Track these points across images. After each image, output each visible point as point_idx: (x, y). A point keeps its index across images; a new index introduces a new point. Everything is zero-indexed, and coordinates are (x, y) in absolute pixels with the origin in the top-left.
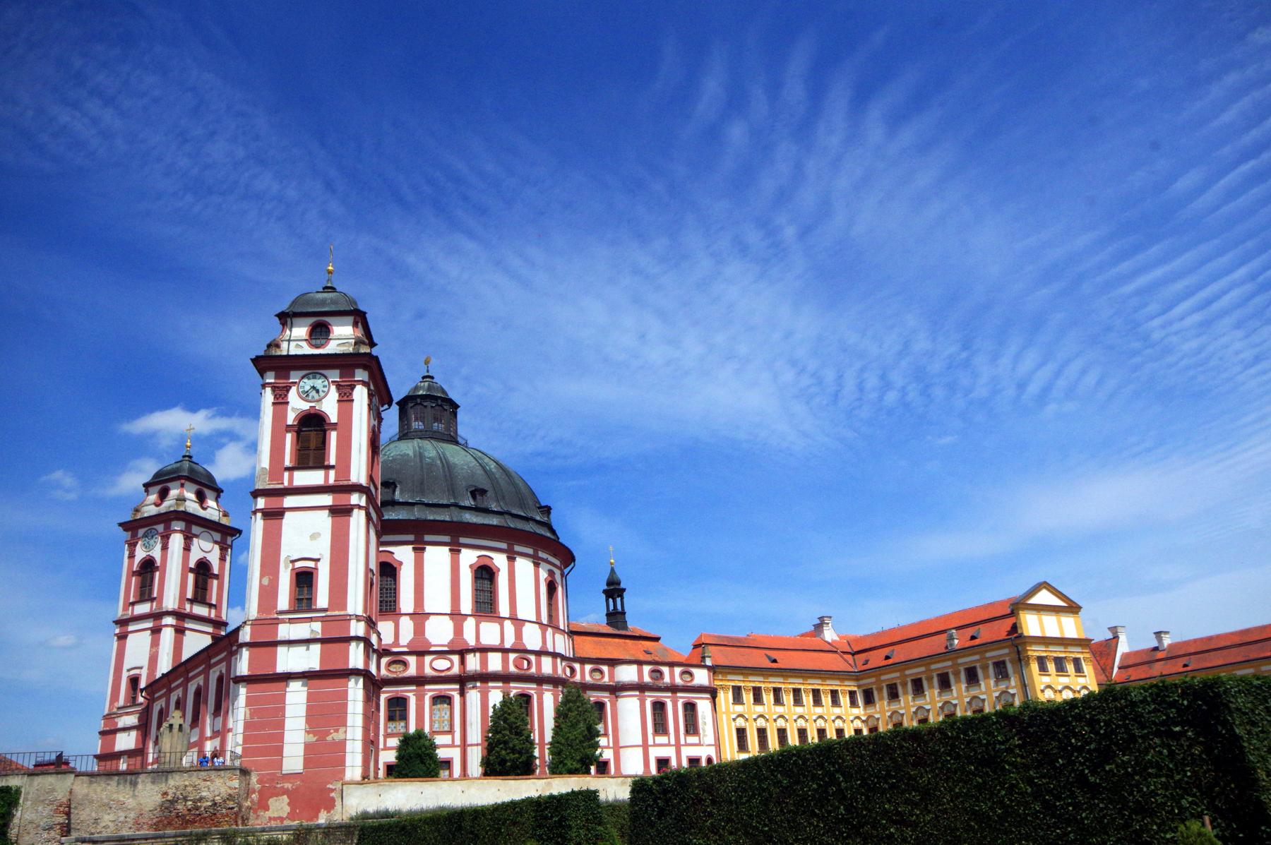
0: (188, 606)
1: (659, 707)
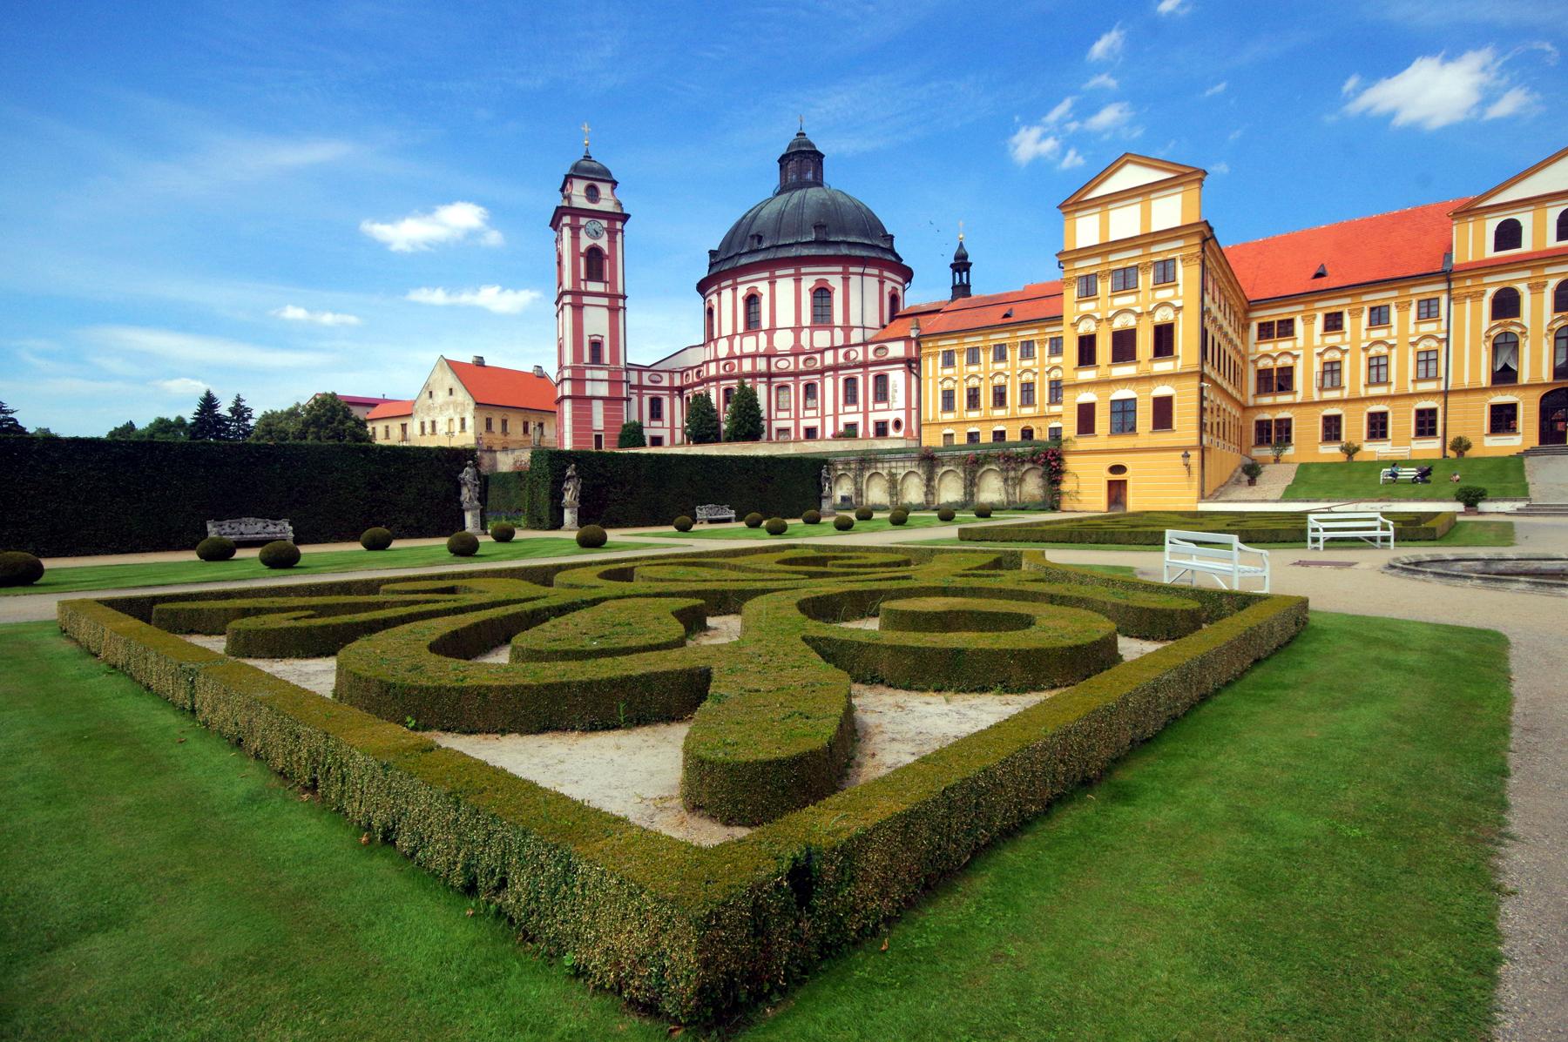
1: (850, 383)
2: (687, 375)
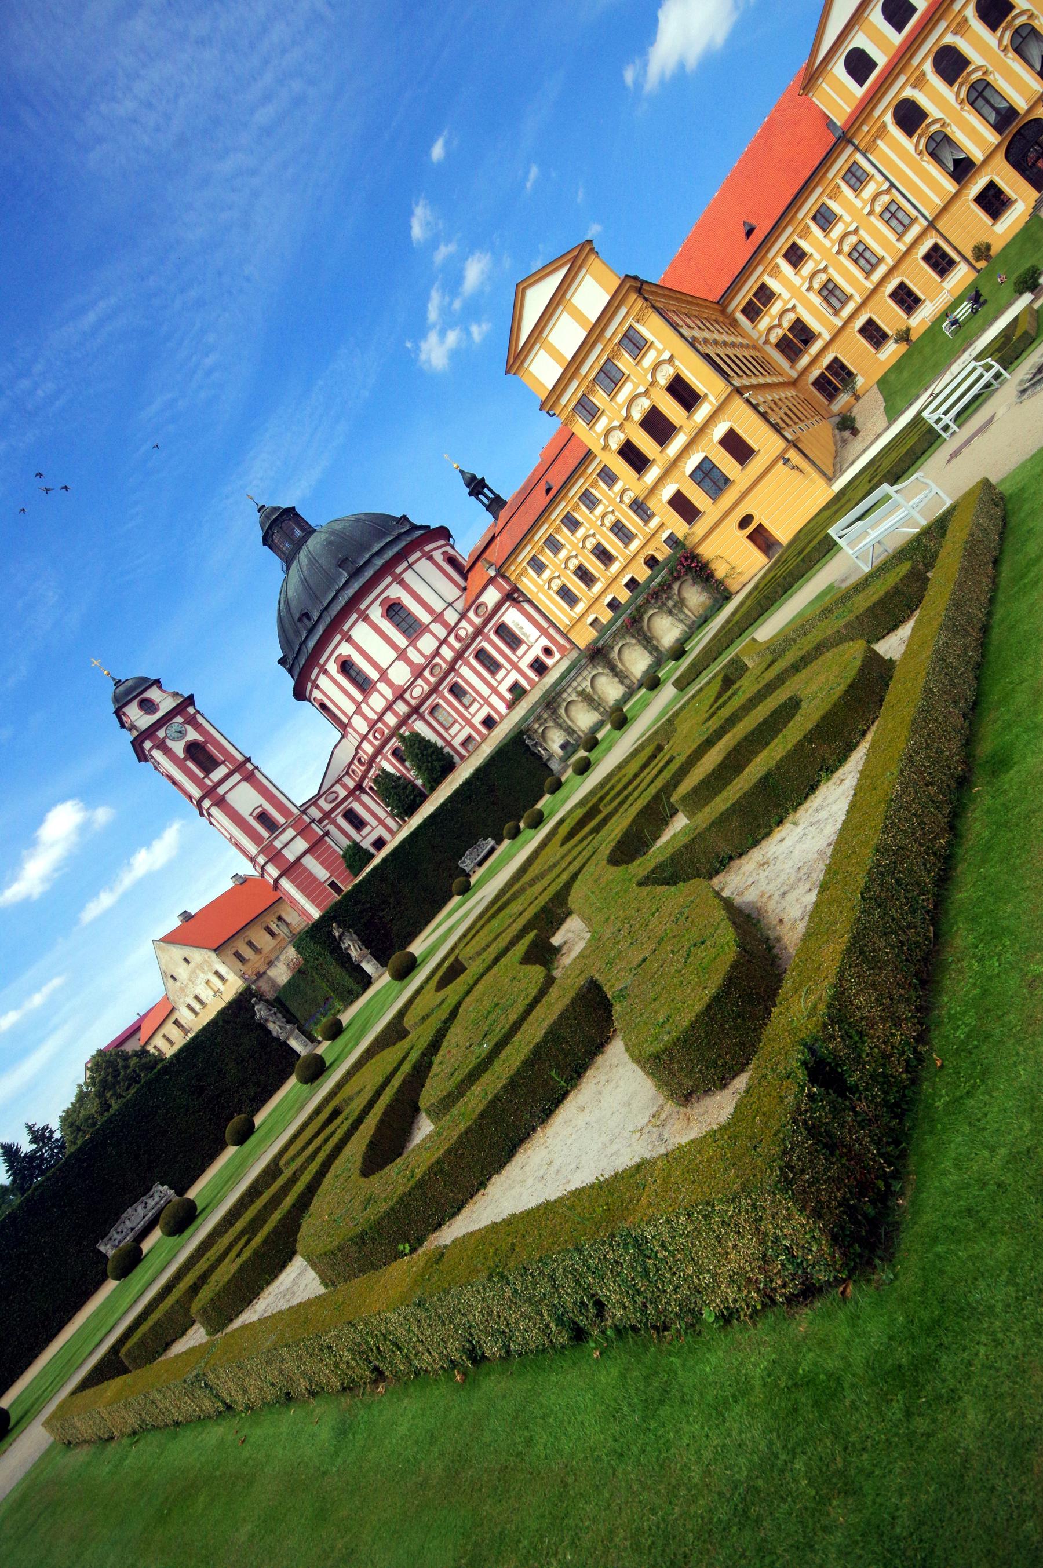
1: (482, 656)
2: (353, 771)
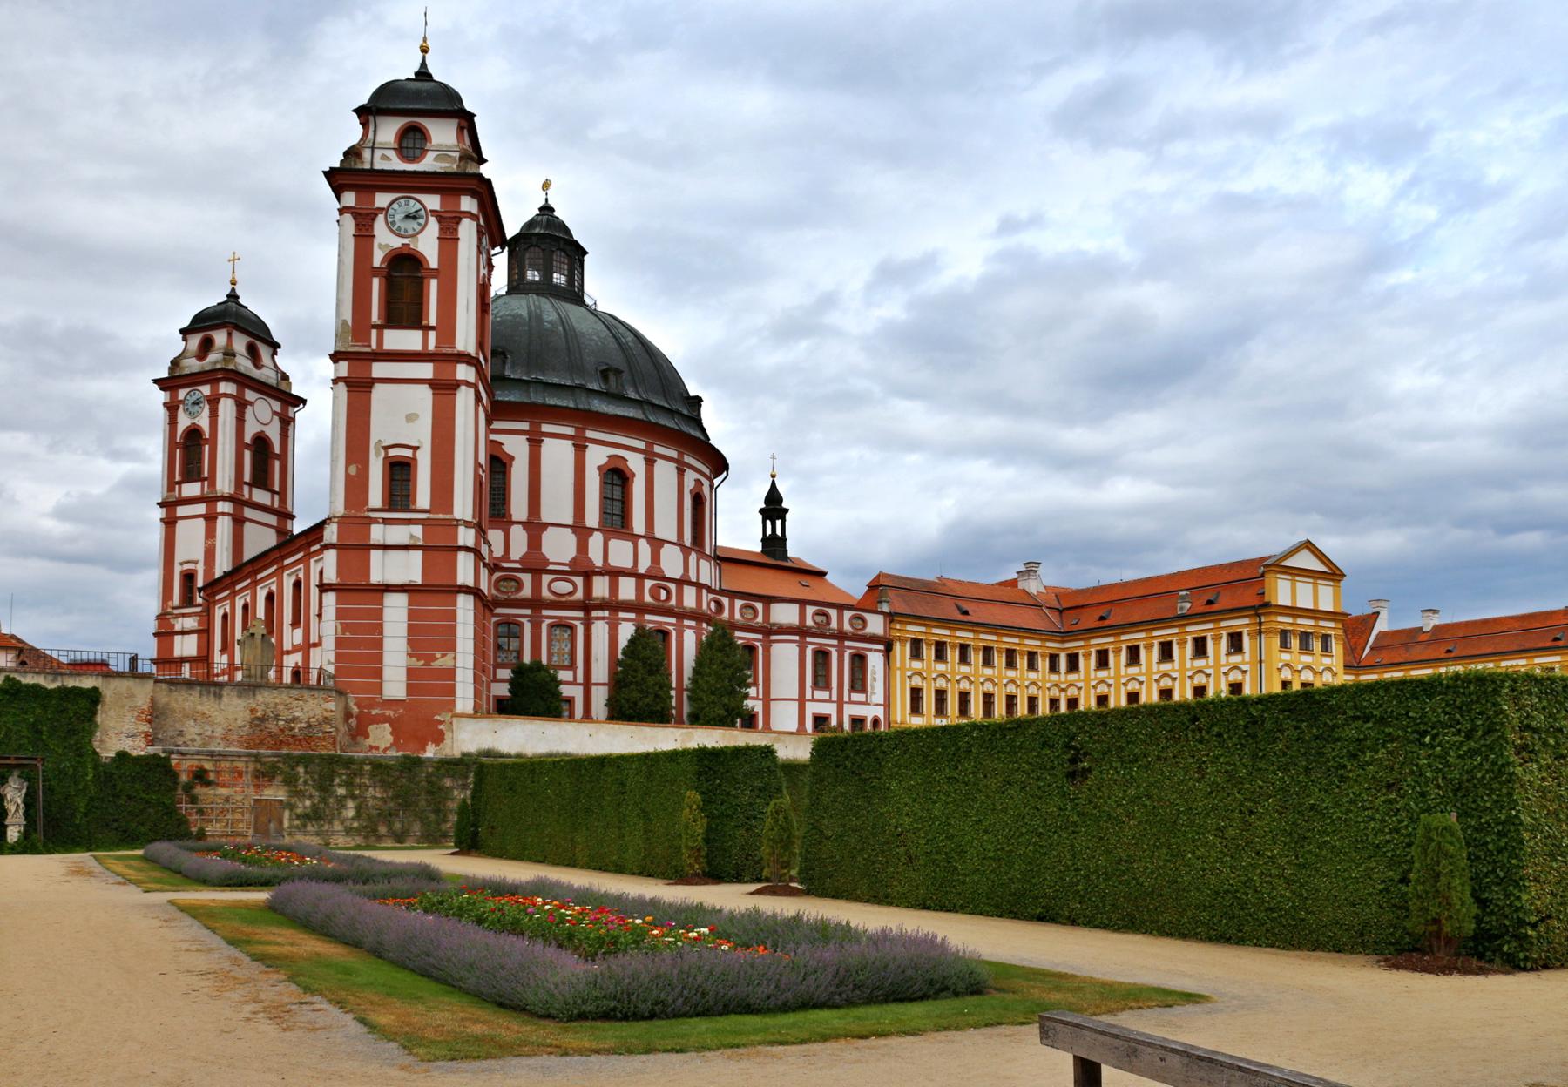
0: (246, 489)
1: (822, 656)
